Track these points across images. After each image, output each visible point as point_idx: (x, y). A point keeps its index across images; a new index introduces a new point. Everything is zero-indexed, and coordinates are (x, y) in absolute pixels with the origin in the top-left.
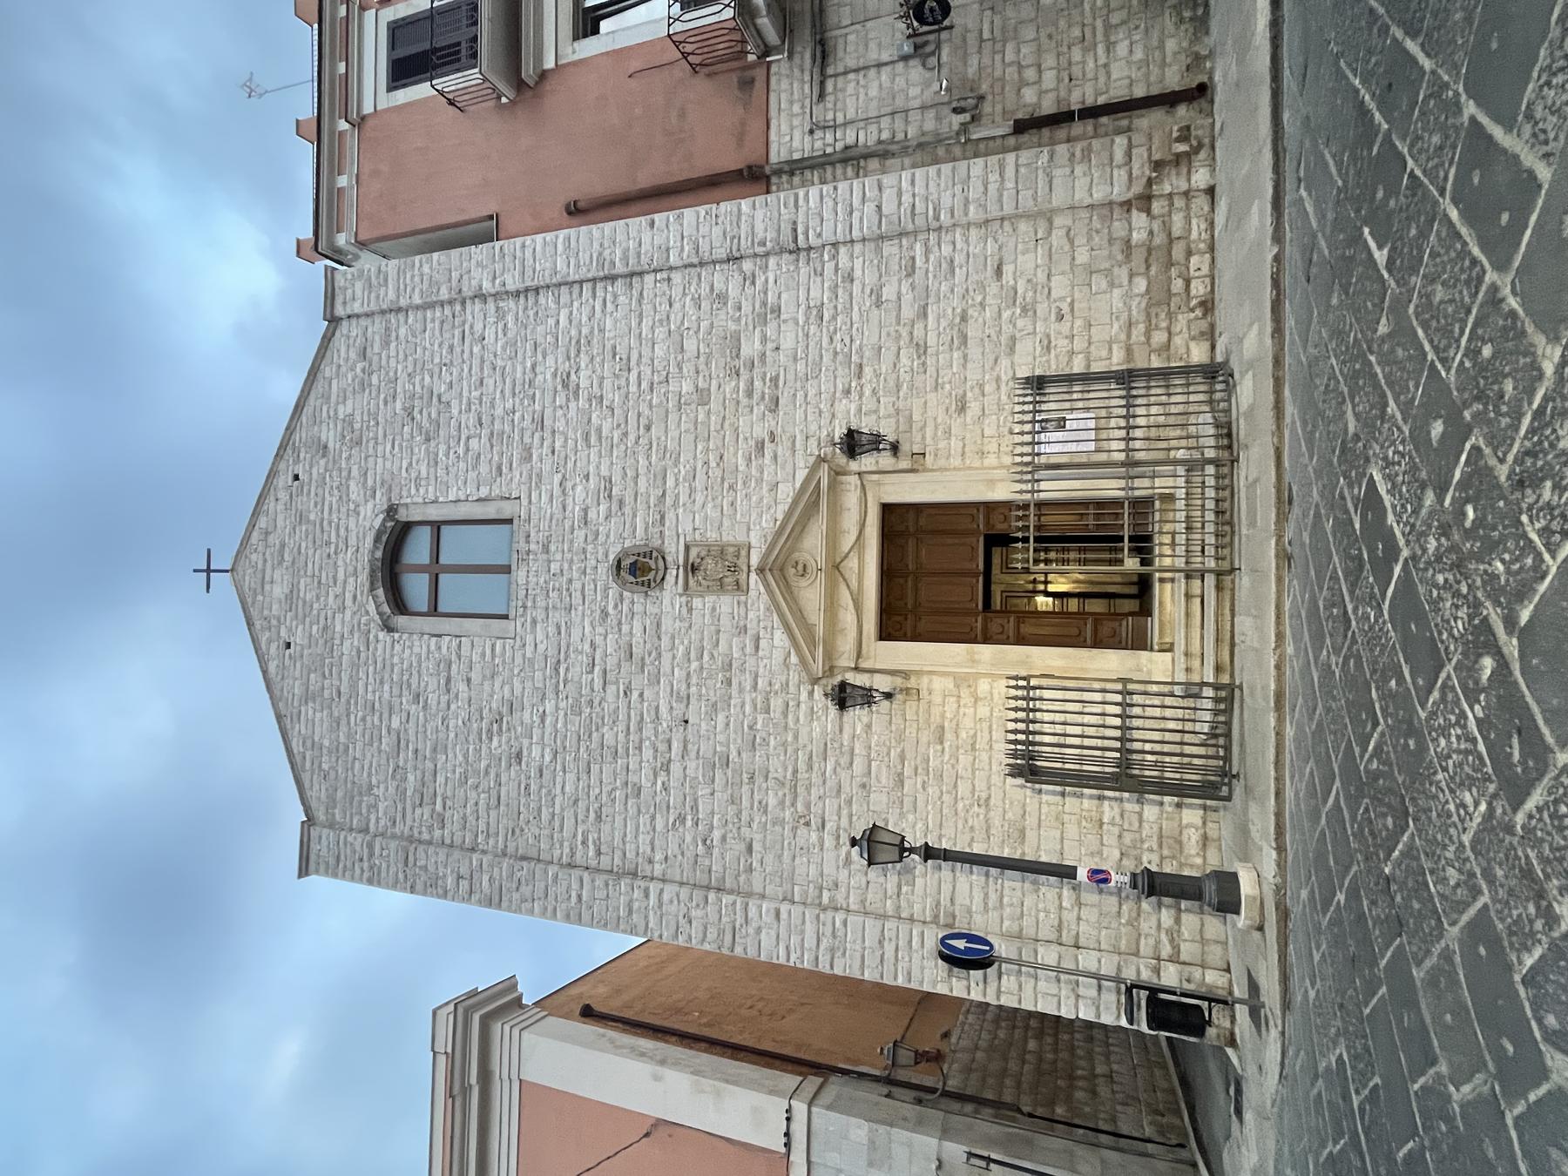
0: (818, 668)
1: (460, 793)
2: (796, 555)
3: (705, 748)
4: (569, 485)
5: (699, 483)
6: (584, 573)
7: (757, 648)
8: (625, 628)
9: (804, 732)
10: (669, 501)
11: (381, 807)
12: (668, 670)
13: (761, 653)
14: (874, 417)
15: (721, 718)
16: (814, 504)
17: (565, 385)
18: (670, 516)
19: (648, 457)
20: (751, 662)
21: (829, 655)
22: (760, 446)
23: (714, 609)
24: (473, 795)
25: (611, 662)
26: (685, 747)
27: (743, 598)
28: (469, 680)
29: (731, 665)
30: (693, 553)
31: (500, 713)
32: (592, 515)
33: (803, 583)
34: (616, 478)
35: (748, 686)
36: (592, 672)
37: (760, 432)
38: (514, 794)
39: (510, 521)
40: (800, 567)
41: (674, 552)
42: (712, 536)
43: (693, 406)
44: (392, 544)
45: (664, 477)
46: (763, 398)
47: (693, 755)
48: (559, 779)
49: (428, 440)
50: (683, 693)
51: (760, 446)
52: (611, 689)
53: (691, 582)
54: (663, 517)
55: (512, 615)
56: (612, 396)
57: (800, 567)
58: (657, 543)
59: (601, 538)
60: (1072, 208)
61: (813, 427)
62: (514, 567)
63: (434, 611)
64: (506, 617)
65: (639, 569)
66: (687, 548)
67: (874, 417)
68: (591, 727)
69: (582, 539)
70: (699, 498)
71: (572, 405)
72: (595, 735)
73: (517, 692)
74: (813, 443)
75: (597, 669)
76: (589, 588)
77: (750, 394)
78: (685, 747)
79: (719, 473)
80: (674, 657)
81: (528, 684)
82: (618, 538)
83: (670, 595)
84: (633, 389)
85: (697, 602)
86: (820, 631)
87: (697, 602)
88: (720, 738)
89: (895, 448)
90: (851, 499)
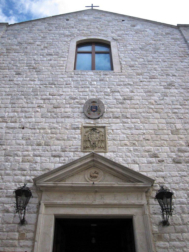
0: (43, 183)
1: (9, 59)
2: (101, 173)
3: (10, 136)
4: (129, 87)
5: (134, 131)
6: (92, 92)
7: (55, 156)
8: (68, 106)
9: (10, 178)
10: (125, 120)
11: (10, 41)
12: (47, 121)
13: (52, 158)
14: (180, 211)
15: (24, 142)
16: (128, 179)
17: (170, 85)
18: (118, 120)
19: (144, 112)
20: (49, 154)
21: (49, 189)
22: (155, 156)
23: (75, 138)
24: (7, 62)
25: (54, 102)
26: (12, 128)
27: (80, 150)
28: (51, 60)
29: (48, 145)
30: (102, 130)
31: (36, 68)
32: (116, 94)
33: (87, 176)
34: (133, 101)
35: (37, 153)
36: (50, 95)
37: (163, 156)
38: (4, 73)
39: (112, 69)
40: (95, 175)
41: (101, 122)
42: (109, 137)
43: (170, 128)
44: (102, 42)
45: (136, 118)
46: (180, 157)
47: (8, 131)
48: (7, 86)
49: (140, 48)
50: (36, 127)
51: (155, 156)
52: (42, 102)
53: (88, 129)
54: (117, 118)
55: (75, 71)
56: (168, 100)
57: (95, 175)
58: (105, 115)
59: (107, 97)
60: (6, 61)
61: (170, 180)
62: (94, 71)
63: (77, 53)
64: (75, 69)
65: (94, 109)
66: (104, 127)
67: (180, 211)
68: (26, 95)
69: (106, 91)
70: (128, 132)
71: (162, 87)
72: (23, 97)
73: (45, 73)
74: (161, 180)
75: (51, 97)
76: (86, 94)
77: (179, 151)
78: (12, 128)
79: (141, 138)
80: (53, 123)
81: (47, 76)
82: (109, 102)
83: (81, 121)
84: (173, 107)
85: (78, 131)
86: (62, 184)
87: (78, 131)
88: (14, 141)
89: (165, 223)
90: (133, 200)
